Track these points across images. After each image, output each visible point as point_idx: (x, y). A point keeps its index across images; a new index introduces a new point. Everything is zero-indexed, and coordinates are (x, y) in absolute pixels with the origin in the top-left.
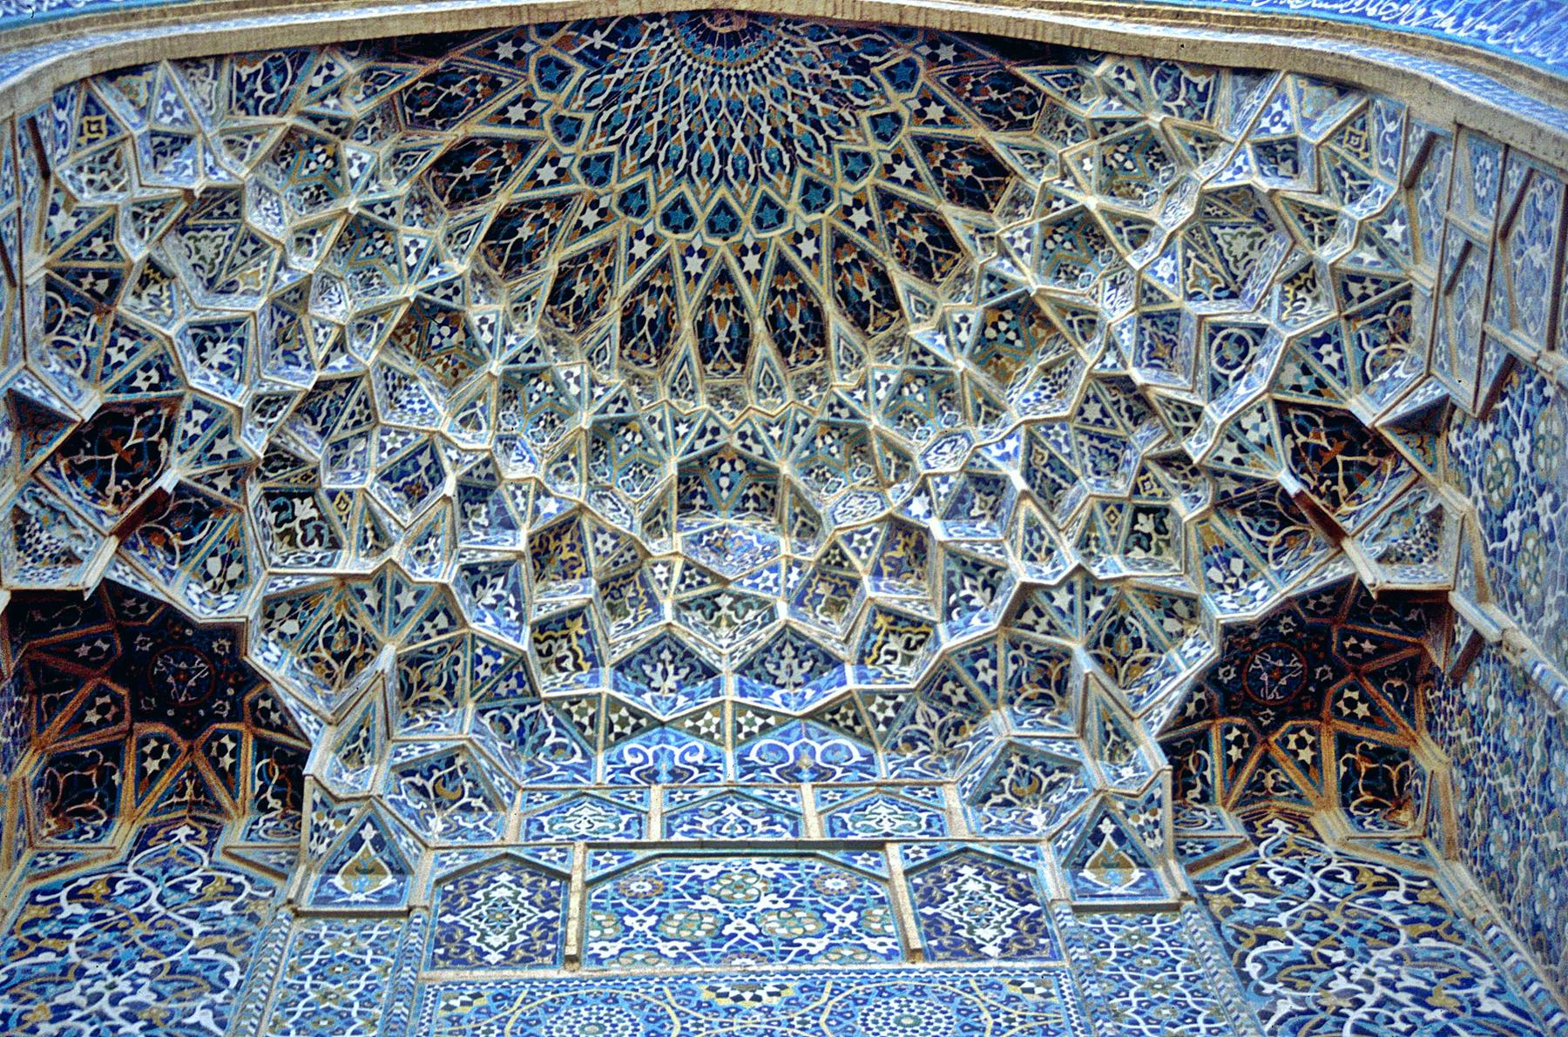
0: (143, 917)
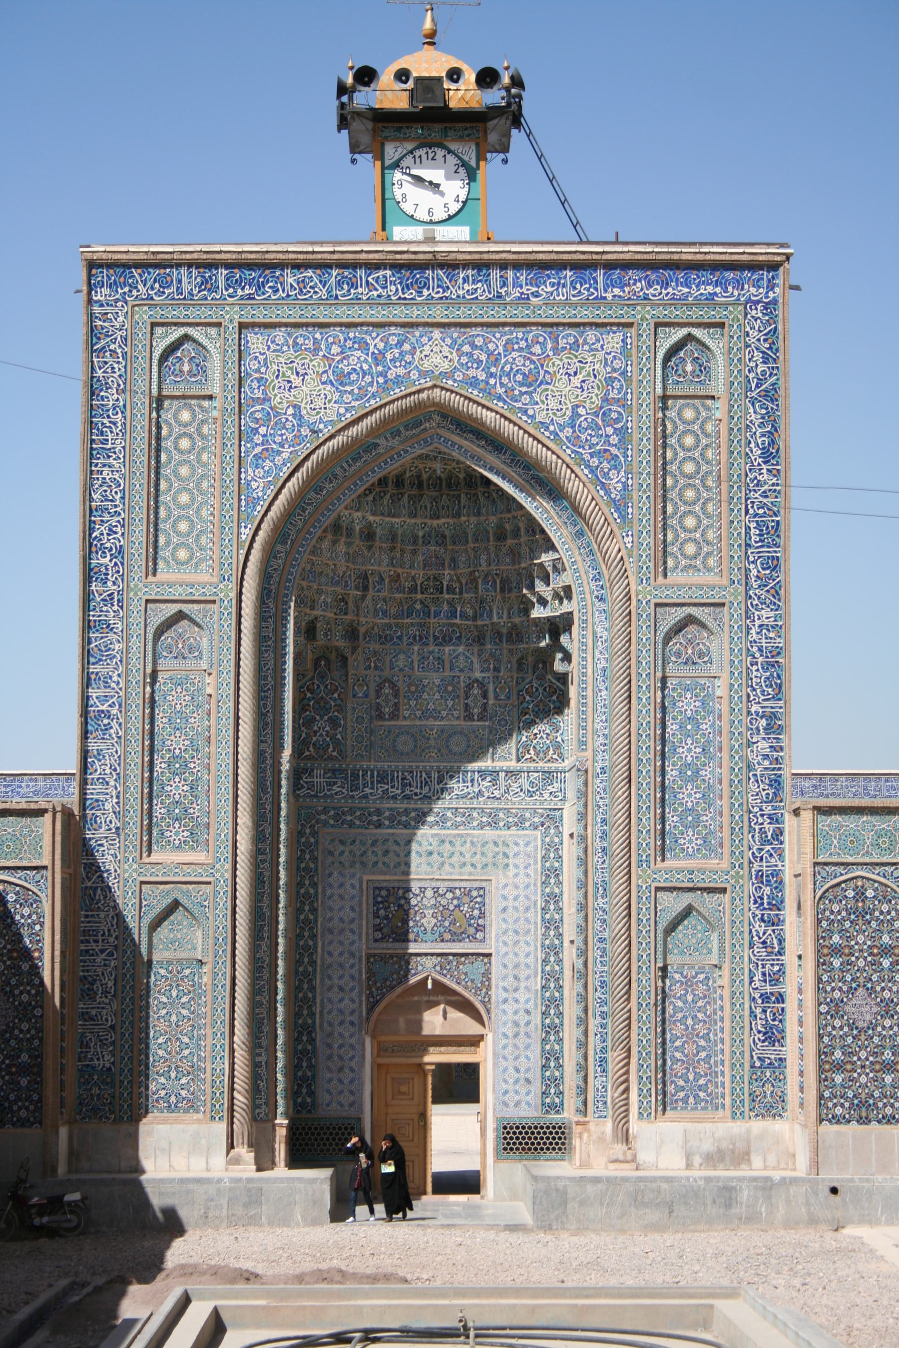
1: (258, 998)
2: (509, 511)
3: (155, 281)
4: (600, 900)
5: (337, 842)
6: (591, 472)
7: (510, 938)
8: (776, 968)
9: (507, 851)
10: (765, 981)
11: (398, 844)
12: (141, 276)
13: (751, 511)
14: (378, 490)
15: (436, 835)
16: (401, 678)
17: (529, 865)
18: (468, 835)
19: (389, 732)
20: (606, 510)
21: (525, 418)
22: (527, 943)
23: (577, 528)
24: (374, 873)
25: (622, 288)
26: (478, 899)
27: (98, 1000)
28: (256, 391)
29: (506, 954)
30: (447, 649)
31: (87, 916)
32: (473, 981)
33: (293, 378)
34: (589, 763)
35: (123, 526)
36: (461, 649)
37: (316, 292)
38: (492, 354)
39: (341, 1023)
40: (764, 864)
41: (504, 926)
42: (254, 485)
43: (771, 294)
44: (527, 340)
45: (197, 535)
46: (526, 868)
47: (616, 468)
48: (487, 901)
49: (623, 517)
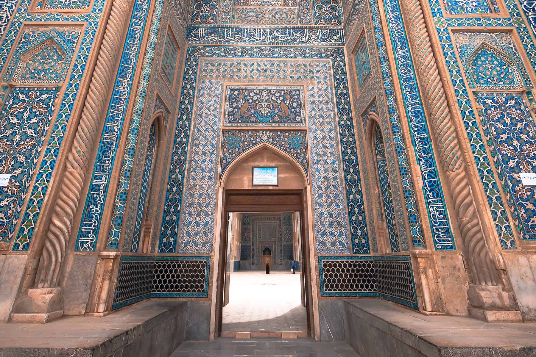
7: (318, 120)
11: (246, 66)
15: (269, 61)
22: (329, 123)
26: (296, 97)
29: (316, 130)
32: (294, 148)
48: (302, 98)
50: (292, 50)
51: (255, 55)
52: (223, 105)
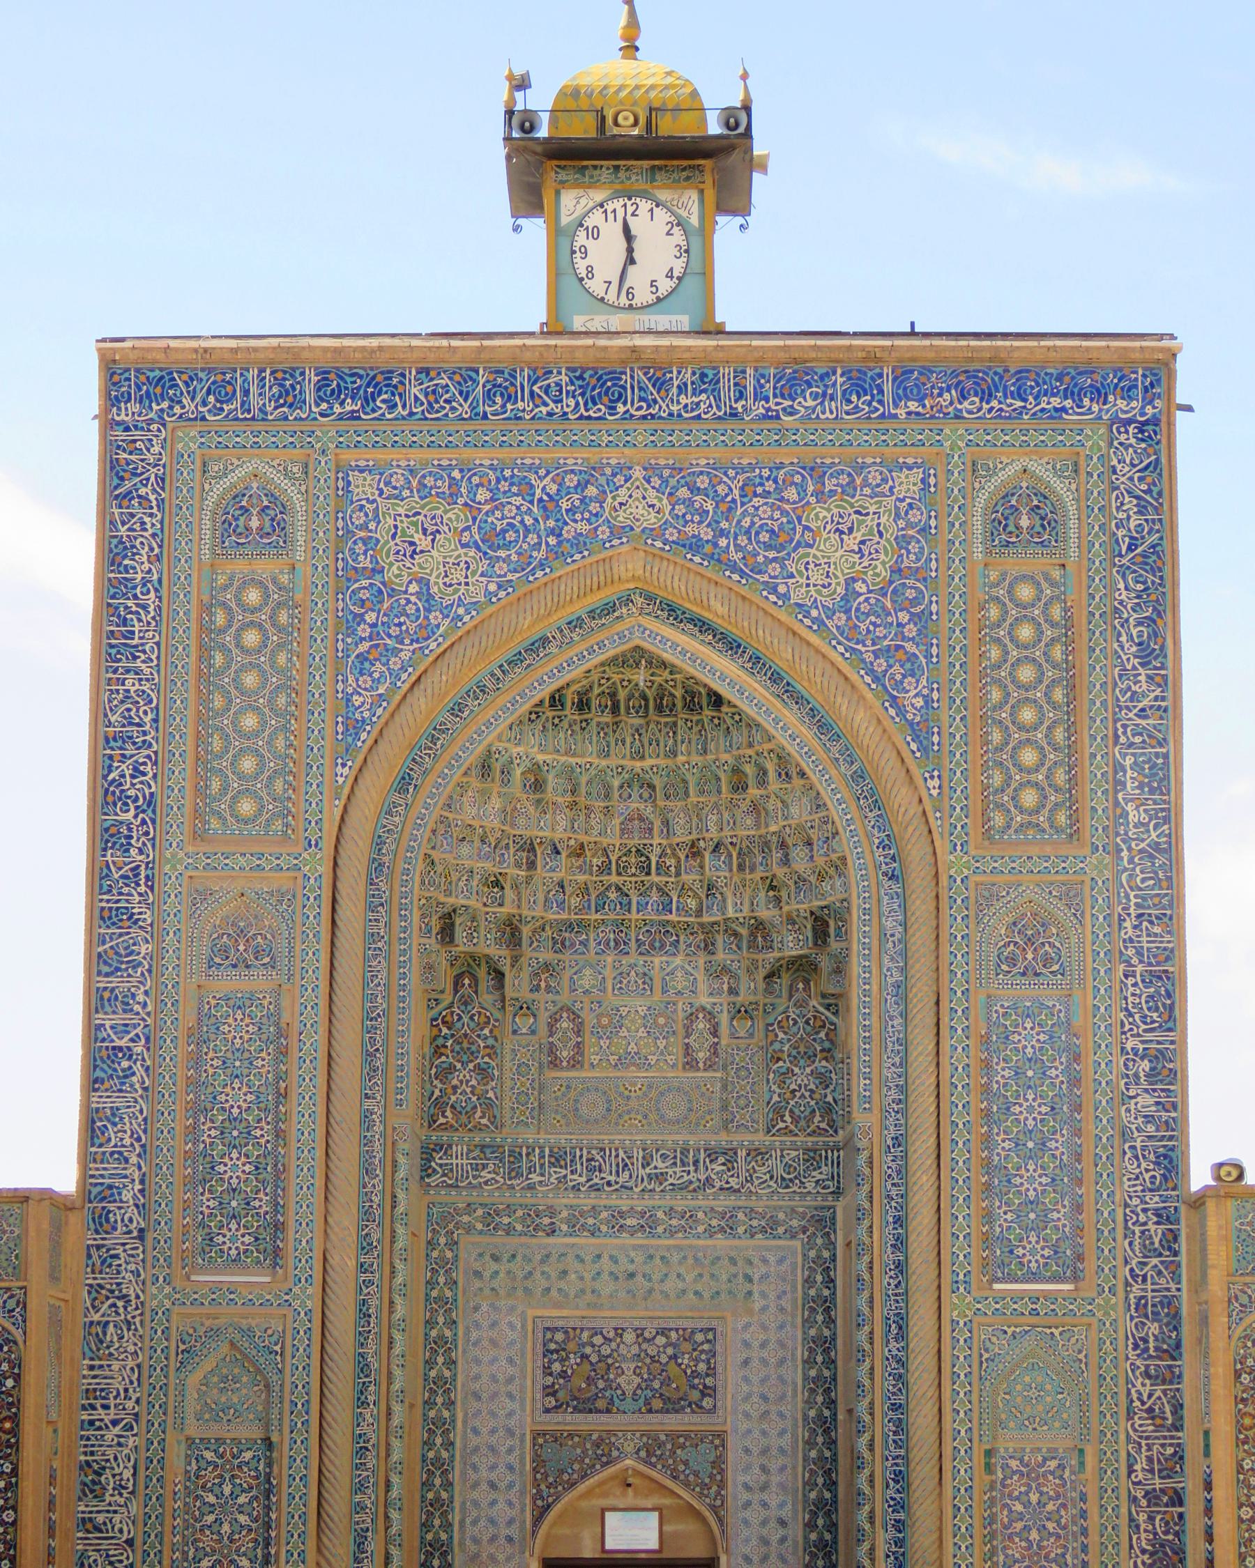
0: (466, 1035)
1: (357, 1498)
2: (750, 745)
3: (208, 393)
4: (893, 1344)
5: (487, 1258)
6: (876, 679)
8: (1170, 1451)
9: (749, 1272)
10: (1152, 1471)
11: (582, 1261)
12: (186, 383)
13: (1123, 739)
14: (550, 714)
16: (587, 1006)
17: (784, 1293)
18: (690, 1246)
19: (568, 1087)
20: (898, 739)
21: (773, 598)
22: (781, 1415)
23: (854, 768)
24: (544, 1307)
25: (921, 400)
26: (706, 1347)
27: (108, 1498)
28: (361, 558)
29: (749, 1431)
30: (657, 960)
31: (92, 1368)
32: (696, 1474)
33: (417, 537)
34: (876, 1129)
35: (156, 763)
36: (678, 961)
37: (453, 409)
38: (723, 500)
39: (493, 1539)
40: (1149, 1287)
41: (745, 1388)
42: (357, 700)
43: (1149, 410)
44: (775, 481)
45: (269, 778)
46: (779, 1297)
47: (913, 676)
48: (718, 1348)
49: (924, 749)
50: (700, 1215)
51: (604, 1228)
52: (529, 1369)
